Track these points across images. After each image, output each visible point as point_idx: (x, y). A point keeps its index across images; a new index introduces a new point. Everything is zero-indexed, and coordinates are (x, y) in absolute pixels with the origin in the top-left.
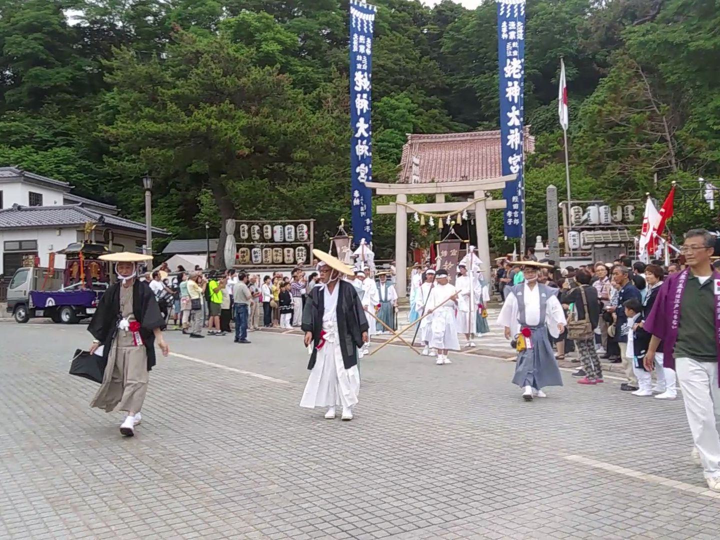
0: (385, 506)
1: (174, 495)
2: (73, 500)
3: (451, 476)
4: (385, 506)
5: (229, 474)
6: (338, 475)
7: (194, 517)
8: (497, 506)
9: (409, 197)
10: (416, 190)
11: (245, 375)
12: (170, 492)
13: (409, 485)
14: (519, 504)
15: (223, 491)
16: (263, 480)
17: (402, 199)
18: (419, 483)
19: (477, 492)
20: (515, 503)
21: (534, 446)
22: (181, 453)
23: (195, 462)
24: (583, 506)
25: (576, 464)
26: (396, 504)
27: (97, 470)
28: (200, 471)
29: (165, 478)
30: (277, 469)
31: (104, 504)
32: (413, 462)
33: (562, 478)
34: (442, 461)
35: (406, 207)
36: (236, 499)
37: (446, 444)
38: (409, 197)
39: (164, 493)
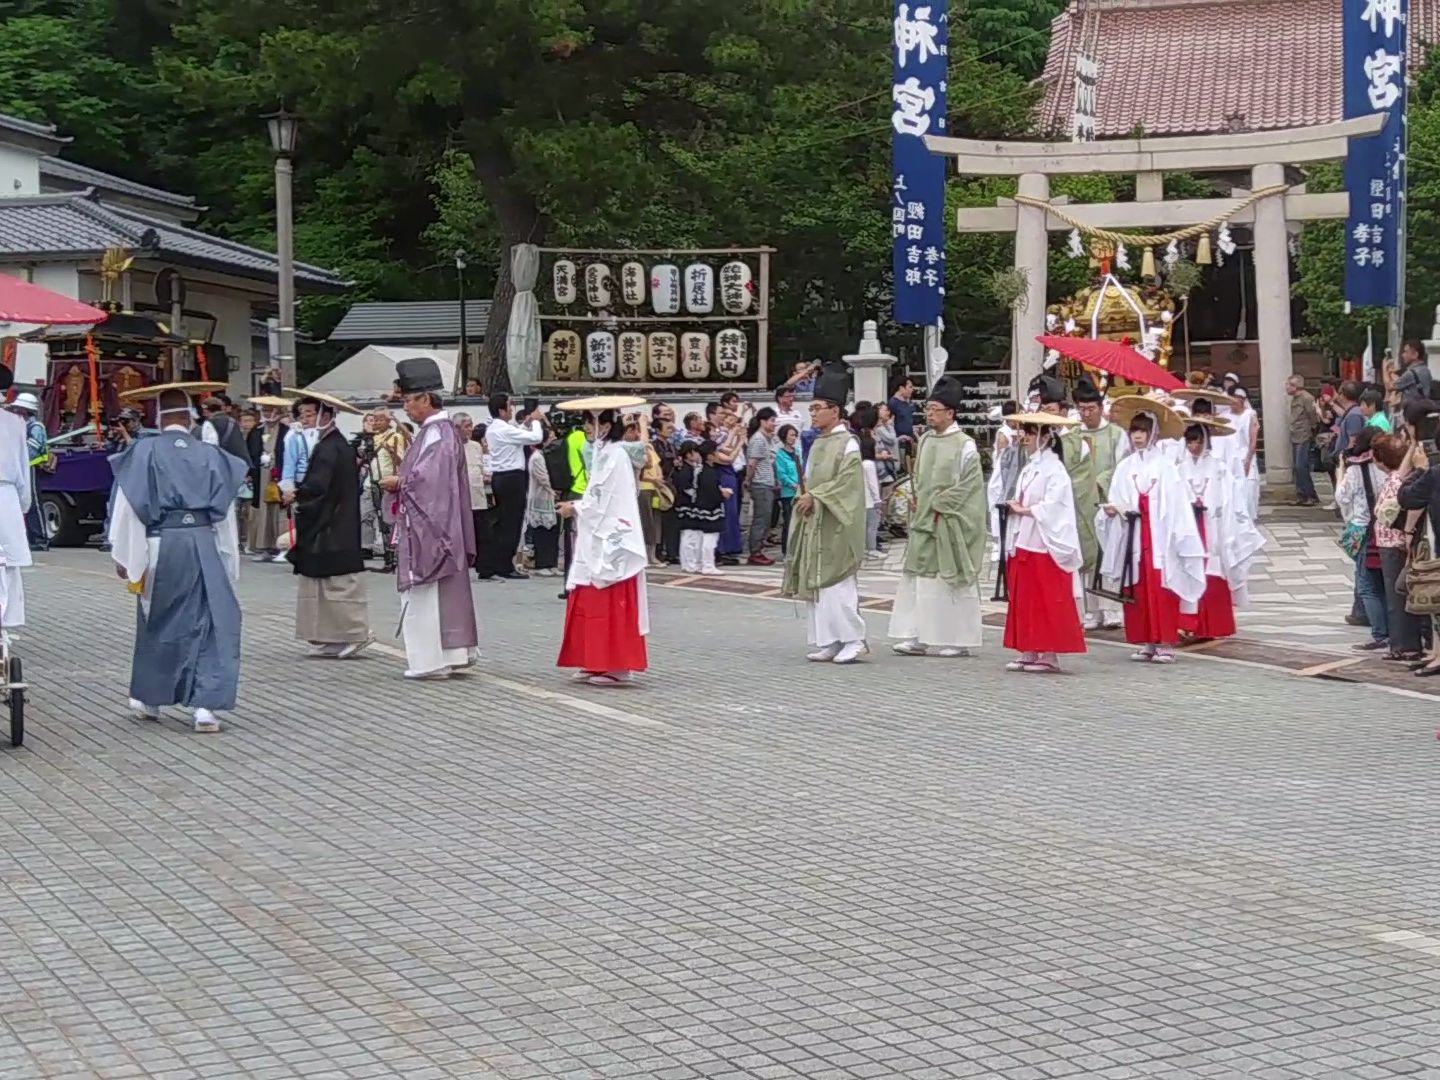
0: (863, 1043)
1: (318, 1006)
2: (61, 1011)
3: (1057, 975)
4: (863, 1043)
5: (468, 956)
6: (753, 965)
7: (365, 1058)
8: (1157, 1049)
9: (1057, 183)
10: (1078, 158)
11: (543, 701)
12: (309, 998)
13: (938, 993)
14: (1218, 1046)
15: (449, 999)
16: (557, 973)
17: (1033, 188)
18: (966, 990)
19: (1113, 1015)
20: (1207, 1045)
21: (1303, 904)
22: (348, 903)
23: (381, 923)
24: (1387, 1057)
25: (1398, 952)
26: (892, 1039)
27: (124, 941)
28: (392, 948)
29: (299, 964)
30: (595, 948)
31: (138, 1022)
32: (962, 937)
33: (1350, 989)
34: (1041, 936)
35: (1046, 211)
36: (478, 1017)
37: (1063, 895)
38: (1057, 183)
39: (295, 1000)
